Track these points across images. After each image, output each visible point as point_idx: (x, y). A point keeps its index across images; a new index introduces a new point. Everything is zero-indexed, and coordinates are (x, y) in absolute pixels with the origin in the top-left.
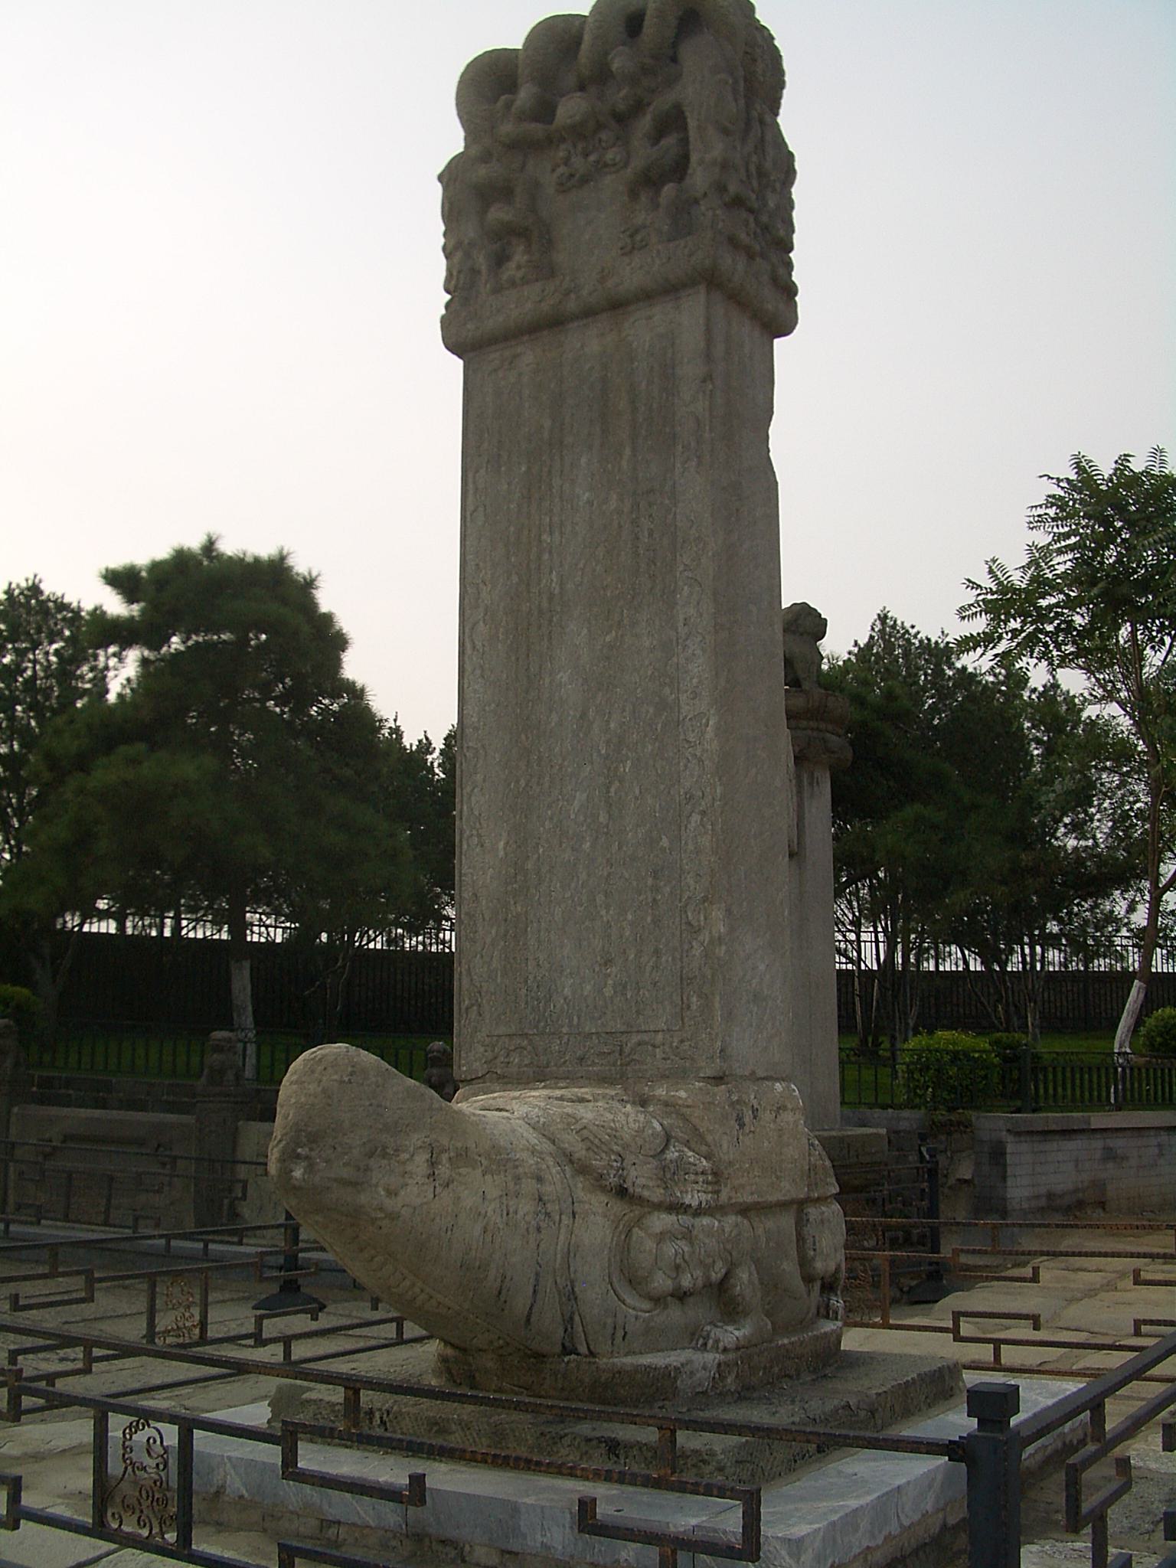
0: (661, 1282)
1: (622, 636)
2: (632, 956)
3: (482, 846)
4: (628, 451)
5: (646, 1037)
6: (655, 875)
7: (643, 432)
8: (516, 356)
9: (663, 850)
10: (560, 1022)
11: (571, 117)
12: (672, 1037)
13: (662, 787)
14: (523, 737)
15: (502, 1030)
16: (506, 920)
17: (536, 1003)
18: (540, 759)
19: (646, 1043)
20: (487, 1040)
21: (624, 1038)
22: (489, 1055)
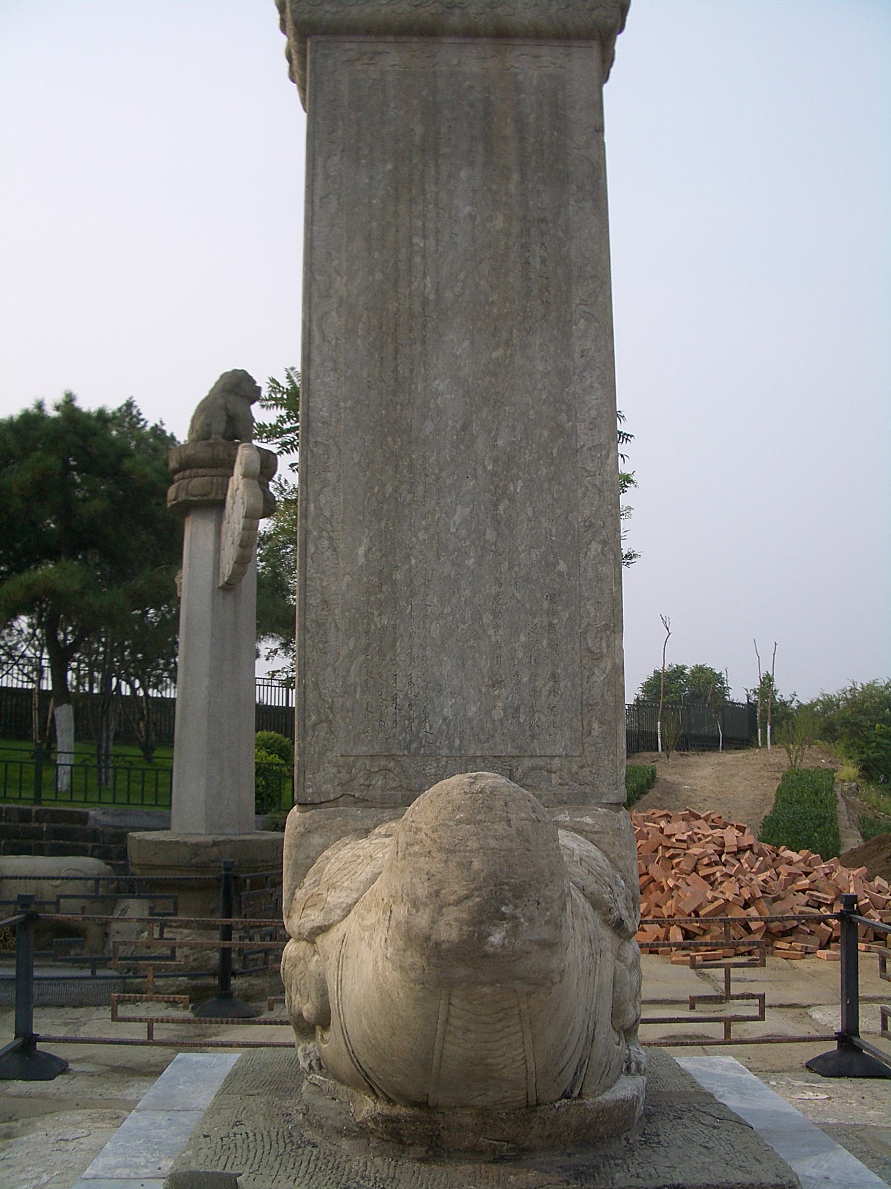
1: (511, 355)
2: (525, 679)
3: (335, 550)
4: (516, 177)
5: (541, 762)
6: (552, 598)
7: (533, 164)
8: (376, 53)
9: (560, 574)
10: (438, 744)
12: (570, 762)
13: (559, 511)
14: (389, 439)
15: (363, 749)
17: (407, 722)
18: (411, 466)
20: (341, 761)
21: (514, 763)
22: (344, 776)
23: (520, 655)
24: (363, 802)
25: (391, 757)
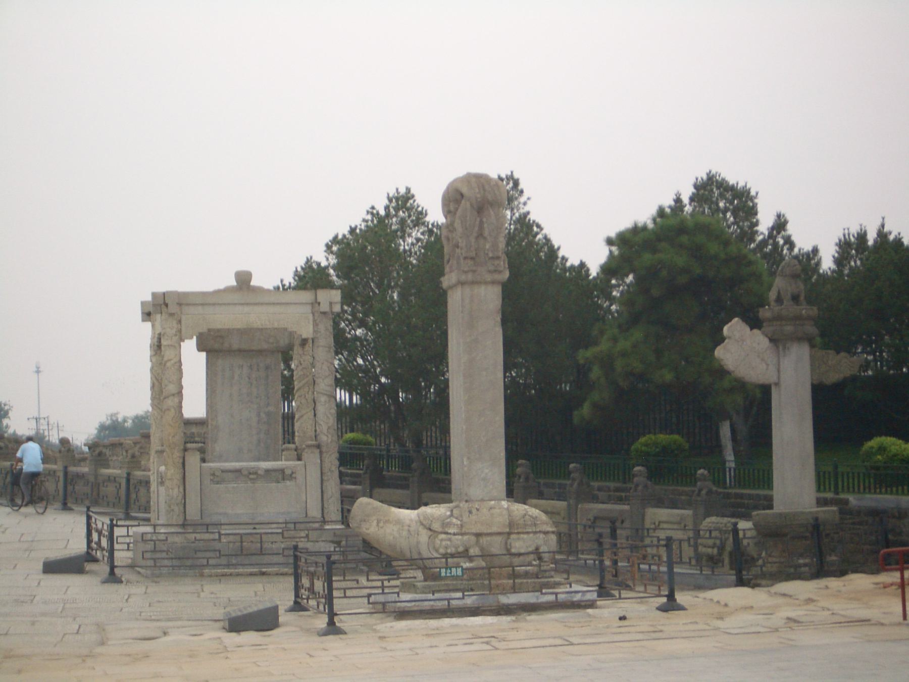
0: (442, 551)
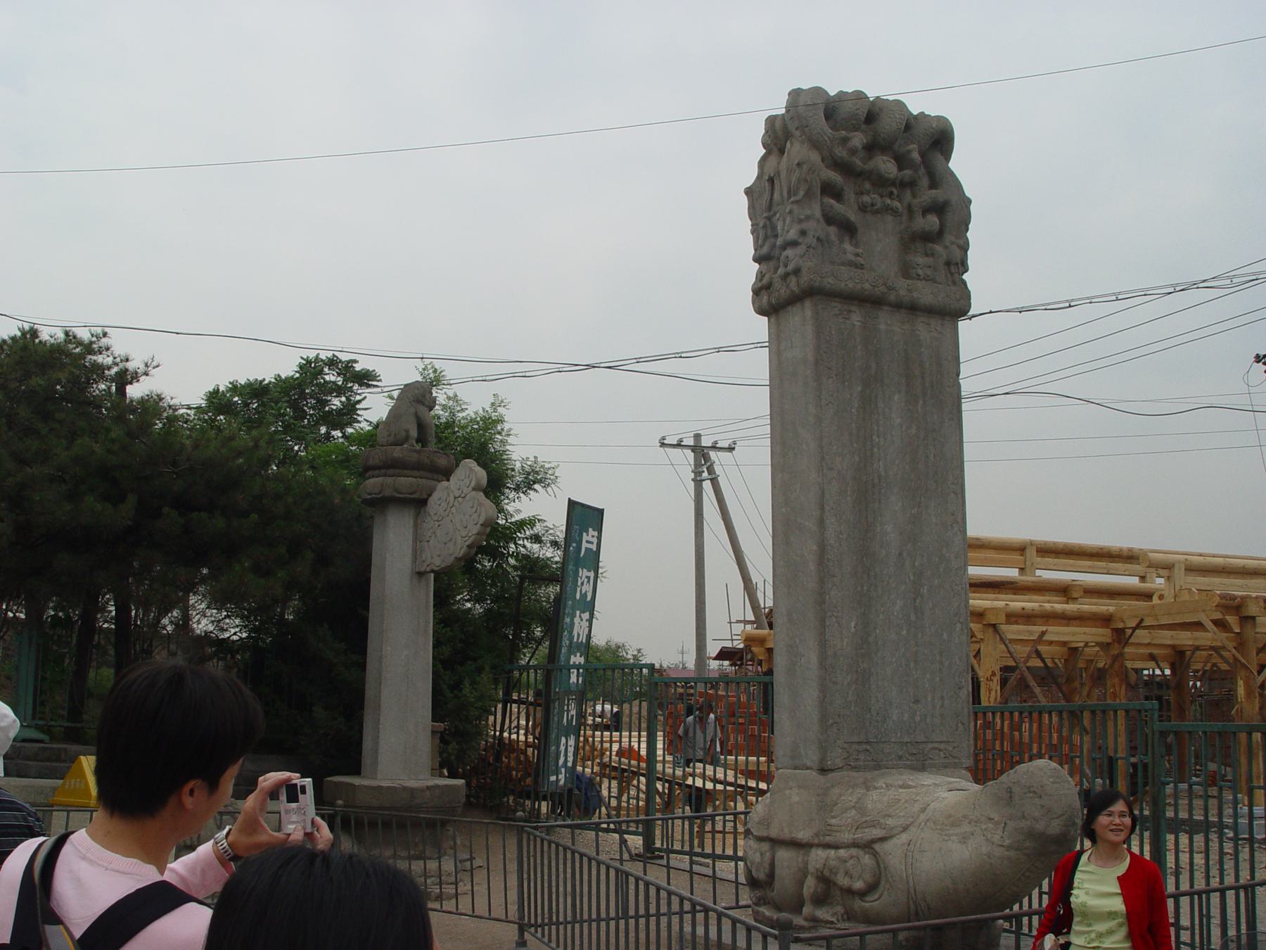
2: (930, 699)
5: (936, 745)
8: (850, 311)
11: (886, 172)
15: (855, 739)
16: (857, 671)
19: (936, 749)
22: (845, 755)
23: (927, 686)
24: (856, 768)
25: (868, 743)
